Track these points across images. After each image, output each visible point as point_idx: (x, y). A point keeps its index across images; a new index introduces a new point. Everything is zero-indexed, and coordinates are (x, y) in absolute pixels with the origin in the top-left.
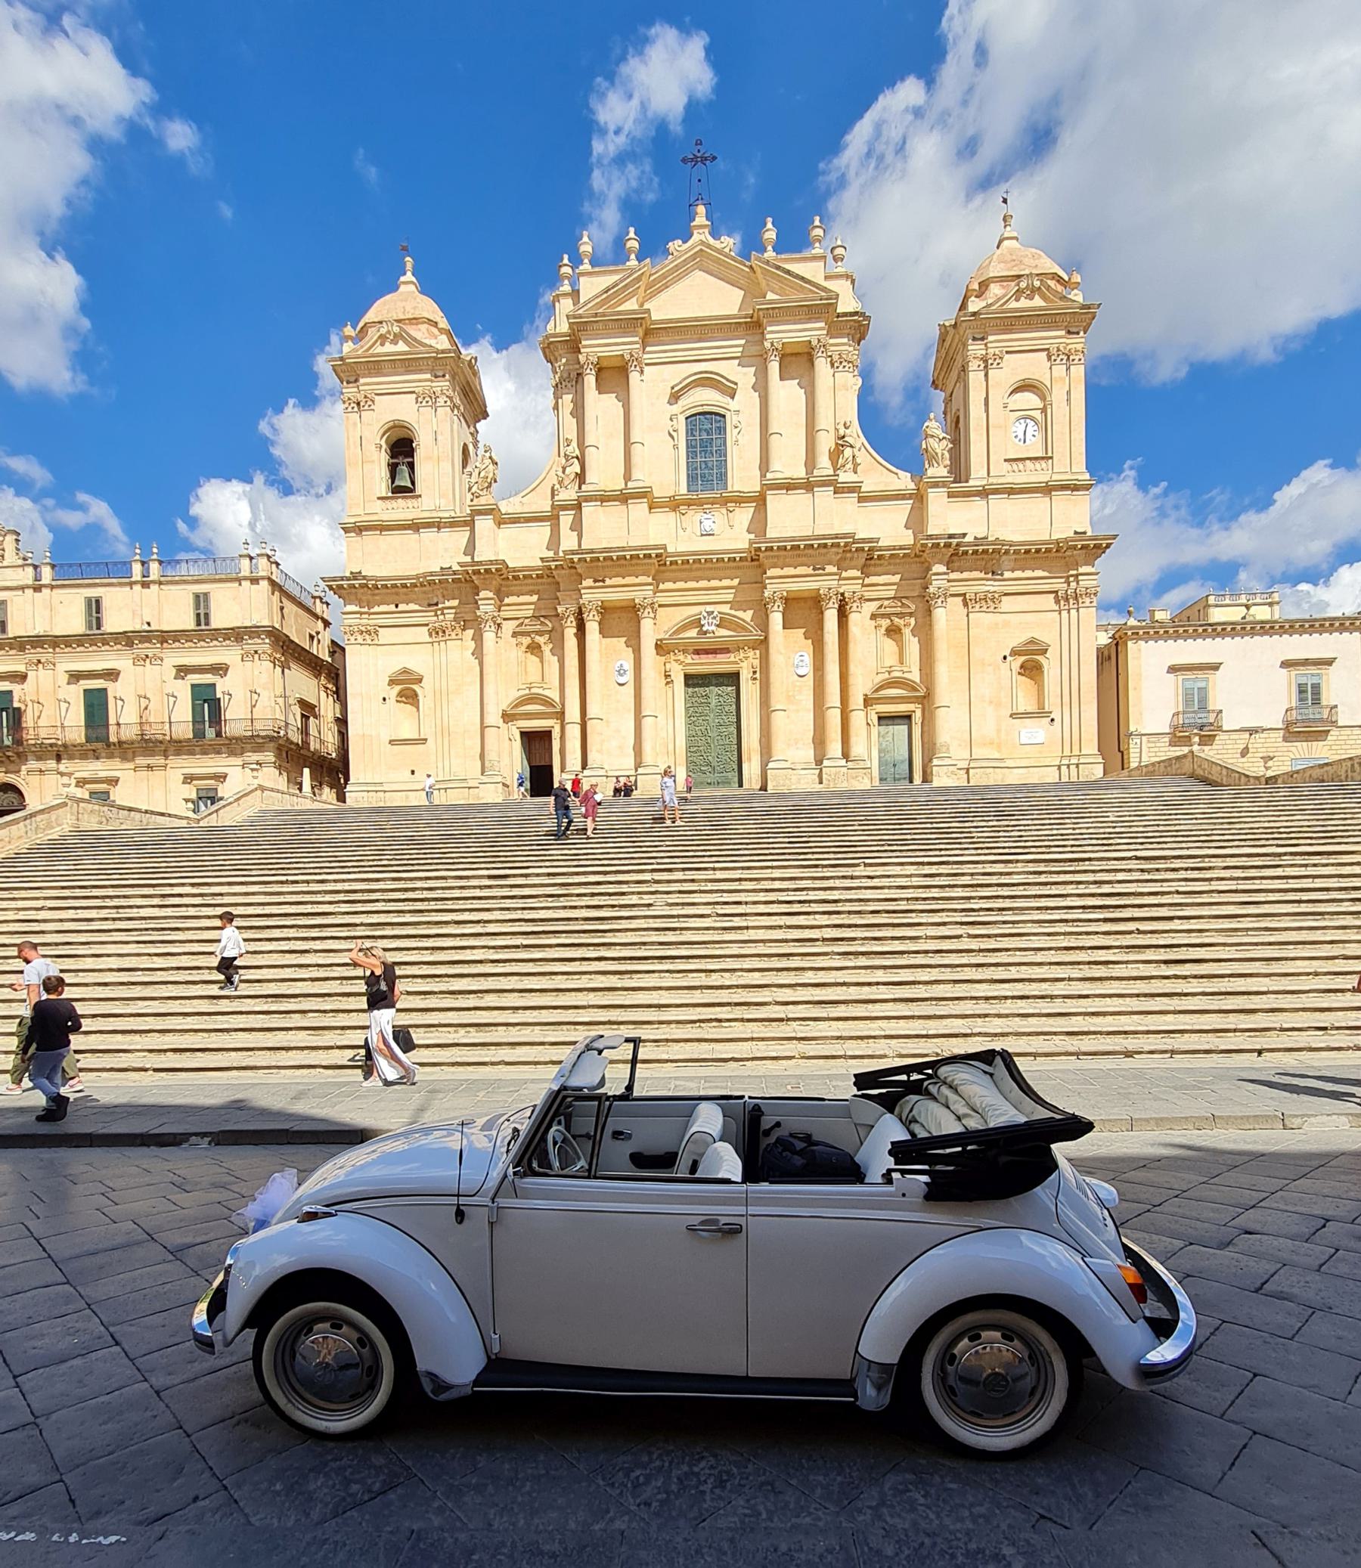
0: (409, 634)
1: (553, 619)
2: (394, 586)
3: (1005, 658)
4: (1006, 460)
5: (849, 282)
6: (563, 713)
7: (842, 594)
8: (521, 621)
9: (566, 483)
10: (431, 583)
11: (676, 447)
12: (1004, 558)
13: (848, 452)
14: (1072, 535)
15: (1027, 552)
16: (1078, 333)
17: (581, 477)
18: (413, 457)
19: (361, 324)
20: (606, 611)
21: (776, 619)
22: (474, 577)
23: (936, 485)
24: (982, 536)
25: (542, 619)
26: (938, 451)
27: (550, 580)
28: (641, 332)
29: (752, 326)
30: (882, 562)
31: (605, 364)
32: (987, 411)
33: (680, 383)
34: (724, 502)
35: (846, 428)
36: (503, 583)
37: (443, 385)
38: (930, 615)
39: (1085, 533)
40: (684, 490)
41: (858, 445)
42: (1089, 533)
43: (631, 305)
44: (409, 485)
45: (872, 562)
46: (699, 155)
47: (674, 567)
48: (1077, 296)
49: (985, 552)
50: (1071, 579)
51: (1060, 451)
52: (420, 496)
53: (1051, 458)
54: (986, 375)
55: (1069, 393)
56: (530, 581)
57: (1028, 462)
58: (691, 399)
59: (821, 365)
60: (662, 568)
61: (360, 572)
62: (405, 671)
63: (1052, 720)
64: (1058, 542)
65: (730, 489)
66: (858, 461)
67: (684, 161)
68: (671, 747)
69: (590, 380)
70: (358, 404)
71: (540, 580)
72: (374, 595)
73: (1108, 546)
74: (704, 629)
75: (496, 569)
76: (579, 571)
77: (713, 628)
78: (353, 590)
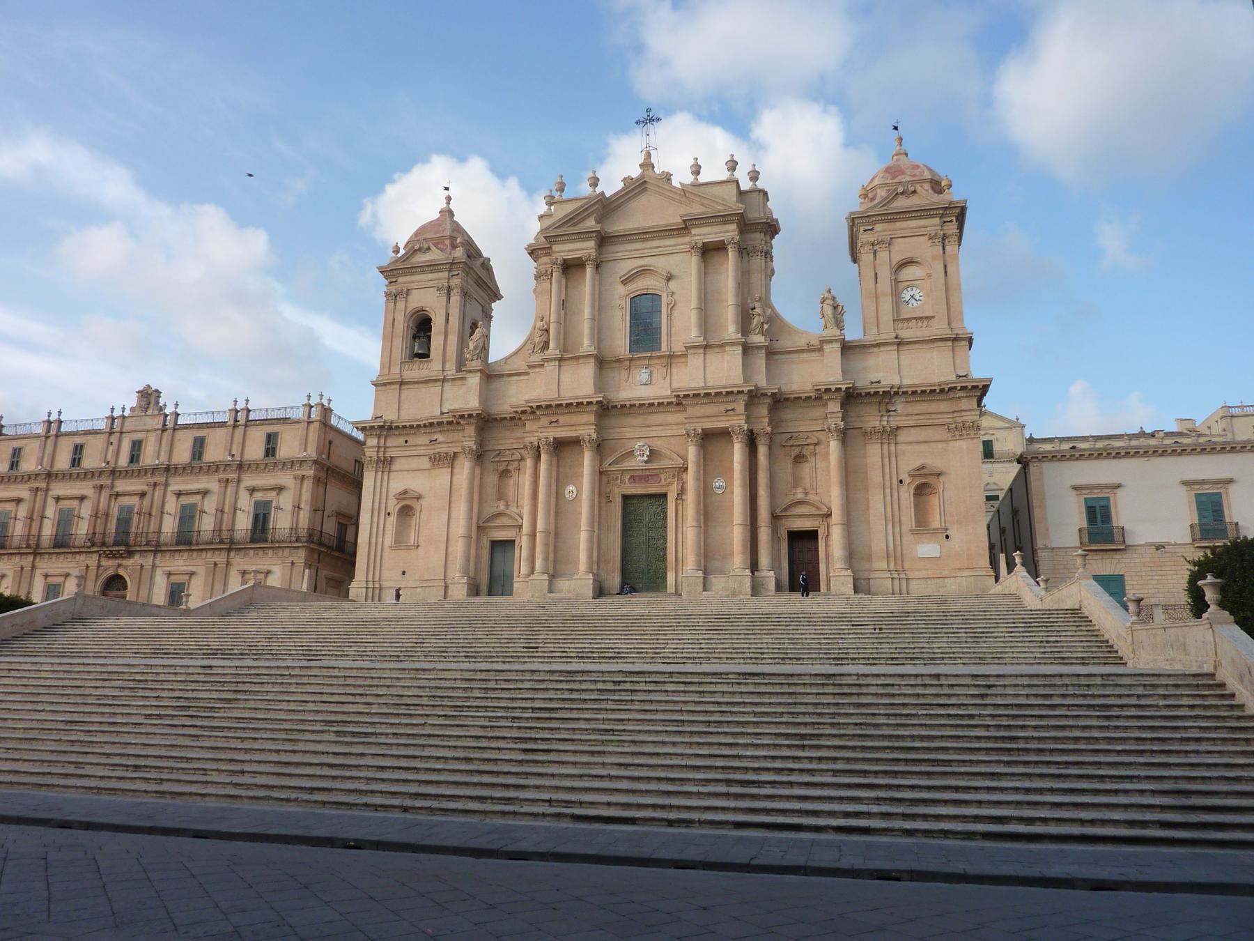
0: (414, 463)
1: (522, 451)
2: (404, 427)
3: (901, 482)
5: (761, 196)
6: (521, 527)
7: (751, 431)
8: (498, 452)
10: (431, 424)
12: (896, 398)
14: (954, 378)
15: (914, 393)
16: (951, 221)
17: (546, 345)
18: (430, 331)
20: (561, 446)
23: (830, 341)
29: (684, 228)
32: (876, 283)
33: (627, 274)
34: (659, 357)
37: (456, 281)
43: (591, 224)
49: (876, 393)
50: (956, 415)
53: (933, 317)
55: (945, 267)
57: (914, 321)
58: (635, 285)
59: (732, 254)
62: (406, 492)
63: (947, 537)
70: (396, 297)
75: (477, 414)
77: (646, 459)
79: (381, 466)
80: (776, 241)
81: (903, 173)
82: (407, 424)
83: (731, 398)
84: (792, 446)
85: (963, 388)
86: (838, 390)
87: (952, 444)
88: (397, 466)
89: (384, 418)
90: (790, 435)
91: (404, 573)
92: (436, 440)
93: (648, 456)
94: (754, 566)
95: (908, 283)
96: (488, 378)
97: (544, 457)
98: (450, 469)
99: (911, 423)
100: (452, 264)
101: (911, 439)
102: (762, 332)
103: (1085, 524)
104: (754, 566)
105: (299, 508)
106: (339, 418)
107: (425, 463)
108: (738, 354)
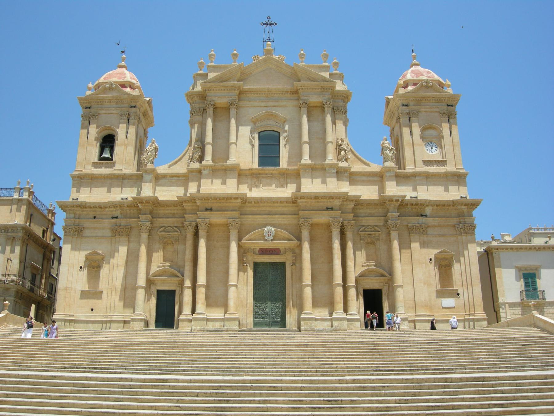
1: (181, 228)
3: (431, 260)
4: (423, 161)
7: (342, 223)
9: (193, 160)
11: (253, 145)
13: (343, 153)
14: (460, 198)
19: (96, 83)
21: (305, 234)
22: (139, 205)
24: (415, 196)
25: (175, 228)
26: (389, 154)
27: (181, 208)
28: (237, 92)
30: (363, 207)
31: (218, 105)
35: (342, 141)
36: (155, 208)
38: (390, 236)
39: (466, 197)
40: (256, 165)
41: (349, 149)
42: (468, 198)
44: (110, 157)
45: (358, 207)
46: (269, 22)
47: (250, 205)
48: (450, 90)
51: (449, 158)
52: (114, 163)
54: (410, 121)
56: (170, 208)
60: (243, 205)
61: (77, 199)
63: (458, 294)
64: (453, 201)
65: (281, 166)
66: (349, 157)
67: (262, 24)
68: (245, 303)
69: (210, 111)
71: (175, 208)
72: (83, 211)
73: (478, 205)
74: (266, 238)
76: (198, 204)
77: (272, 238)
78: (73, 208)
79: (76, 233)
80: (350, 106)
81: (422, 75)
82: (97, 205)
83: (331, 200)
84: (365, 234)
85: (466, 205)
86: (397, 200)
87: (459, 238)
88: (87, 233)
89: (79, 200)
90: (363, 228)
91: (92, 310)
92: (117, 218)
93: (273, 236)
94: (346, 311)
95: (429, 139)
96: (156, 178)
97: (202, 233)
98: (127, 239)
99: (436, 224)
100: (131, 99)
101: (435, 233)
102: (346, 160)
103: (524, 289)
104: (346, 311)
105: (10, 260)
106: (37, 198)
107: (108, 233)
108: (334, 173)
